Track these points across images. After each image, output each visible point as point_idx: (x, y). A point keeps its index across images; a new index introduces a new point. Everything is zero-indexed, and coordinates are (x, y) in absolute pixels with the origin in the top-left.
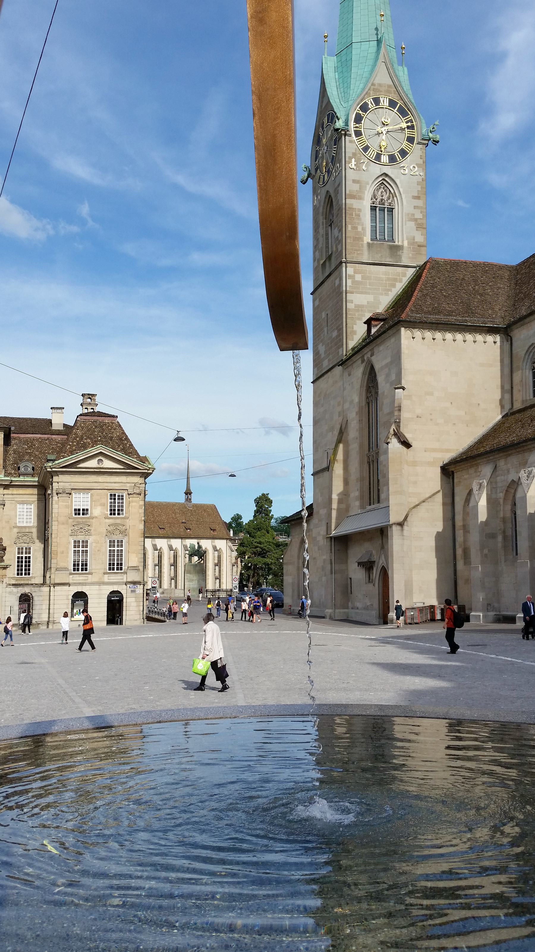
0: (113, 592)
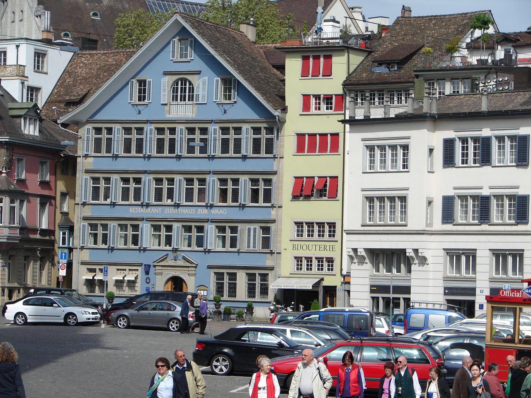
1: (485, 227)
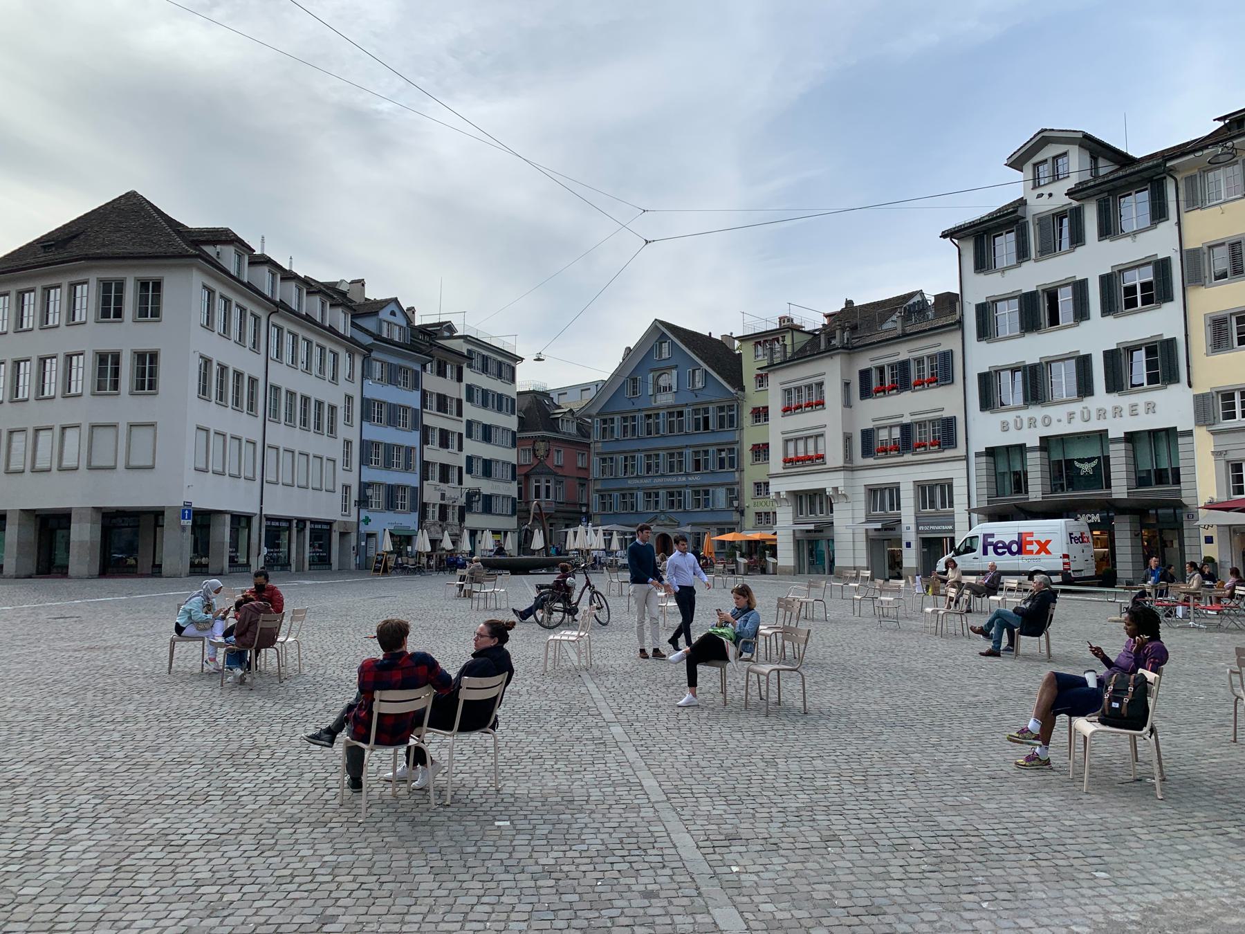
1: (908, 457)
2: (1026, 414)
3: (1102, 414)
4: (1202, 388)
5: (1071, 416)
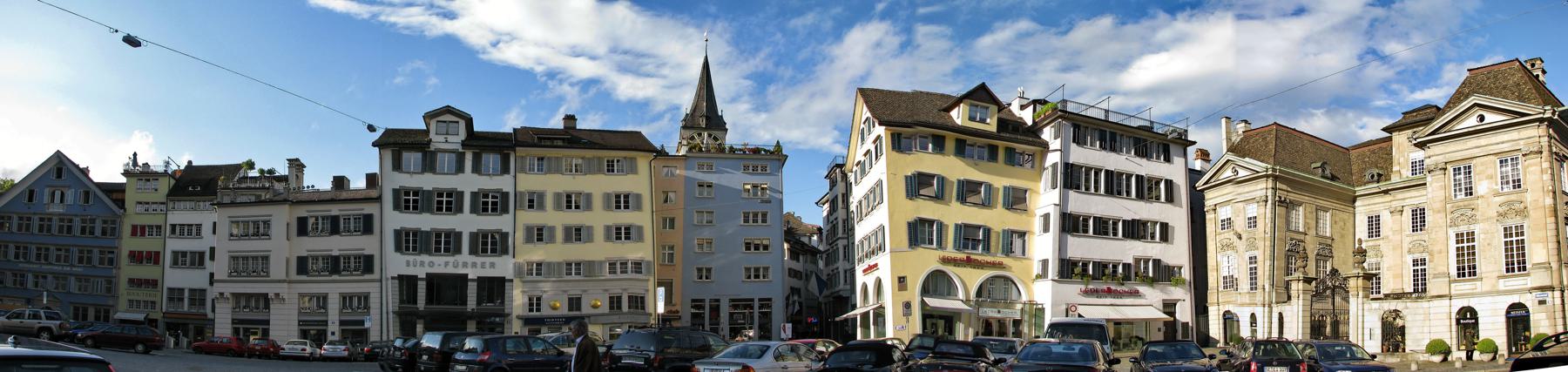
0: (1513, 307)
2: (419, 258)
3: (465, 265)
4: (520, 259)
5: (447, 264)
